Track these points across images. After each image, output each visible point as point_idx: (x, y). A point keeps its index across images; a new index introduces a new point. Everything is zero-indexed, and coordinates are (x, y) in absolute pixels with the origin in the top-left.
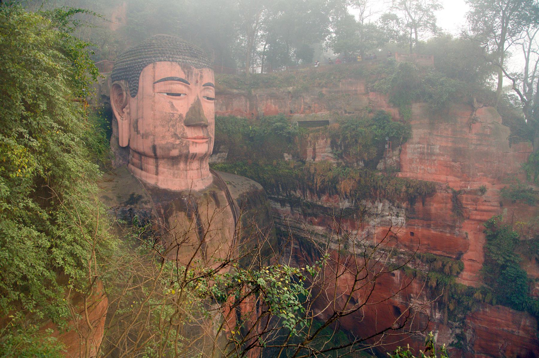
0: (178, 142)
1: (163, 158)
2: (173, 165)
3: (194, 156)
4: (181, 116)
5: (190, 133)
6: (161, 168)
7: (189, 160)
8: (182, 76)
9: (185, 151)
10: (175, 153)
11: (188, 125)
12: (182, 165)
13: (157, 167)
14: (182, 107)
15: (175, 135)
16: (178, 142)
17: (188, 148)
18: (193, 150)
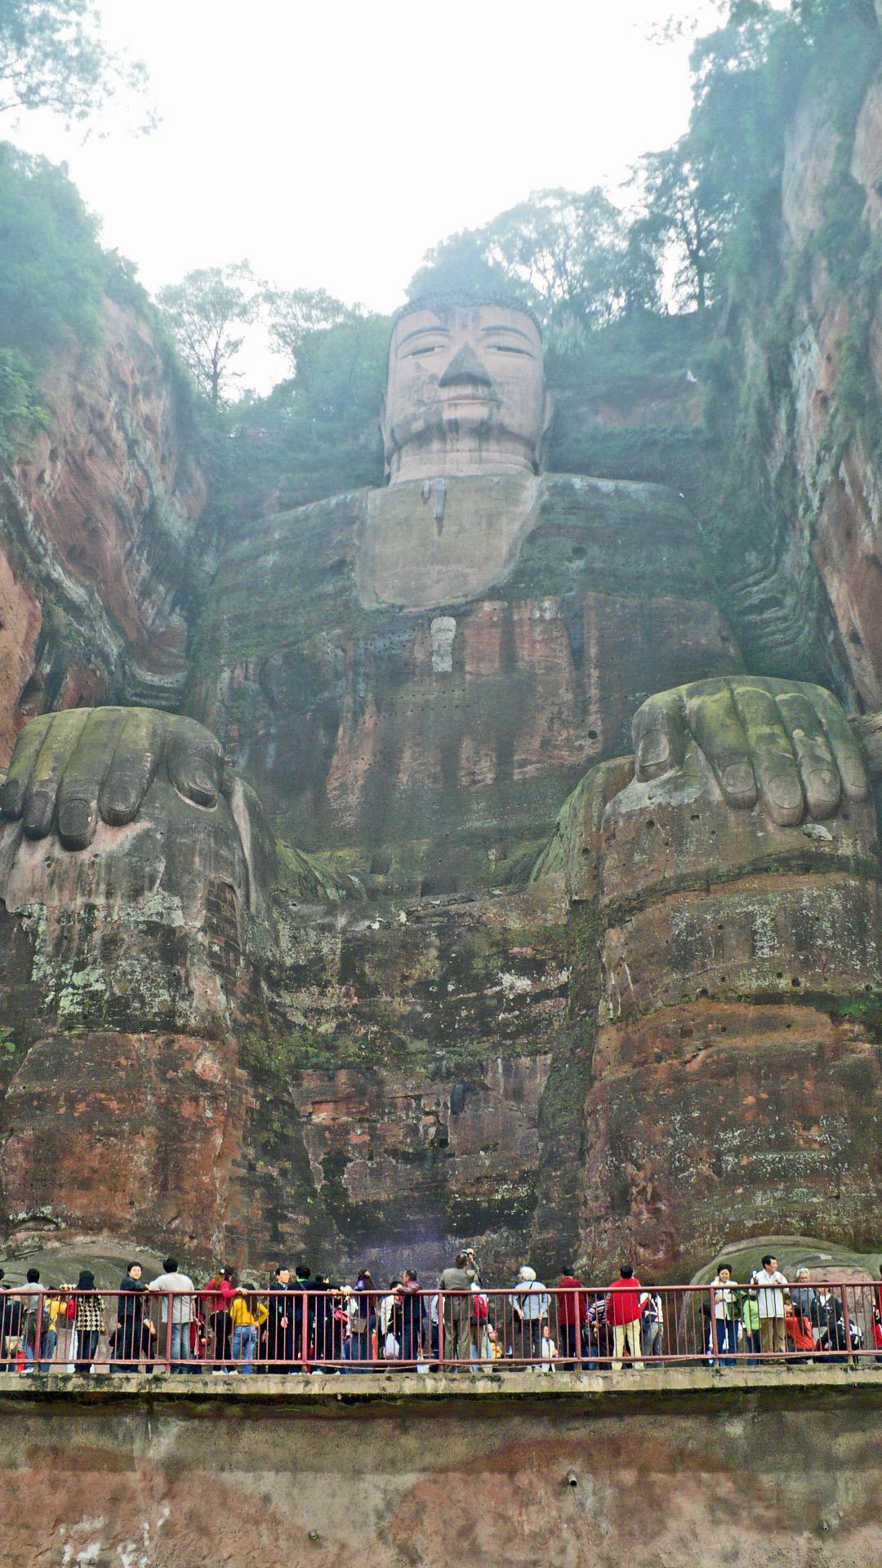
0: (423, 409)
1: (406, 442)
2: (420, 448)
3: (455, 426)
4: (433, 377)
5: (445, 394)
6: (403, 460)
7: (449, 436)
8: (436, 322)
9: (434, 420)
10: (418, 426)
11: (445, 383)
12: (436, 445)
13: (400, 458)
14: (437, 364)
15: (420, 402)
16: (423, 409)
17: (439, 413)
18: (449, 414)
